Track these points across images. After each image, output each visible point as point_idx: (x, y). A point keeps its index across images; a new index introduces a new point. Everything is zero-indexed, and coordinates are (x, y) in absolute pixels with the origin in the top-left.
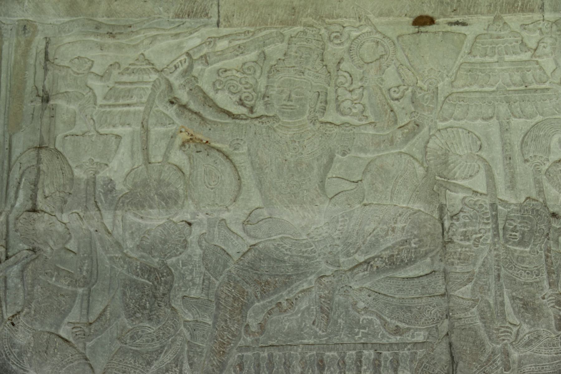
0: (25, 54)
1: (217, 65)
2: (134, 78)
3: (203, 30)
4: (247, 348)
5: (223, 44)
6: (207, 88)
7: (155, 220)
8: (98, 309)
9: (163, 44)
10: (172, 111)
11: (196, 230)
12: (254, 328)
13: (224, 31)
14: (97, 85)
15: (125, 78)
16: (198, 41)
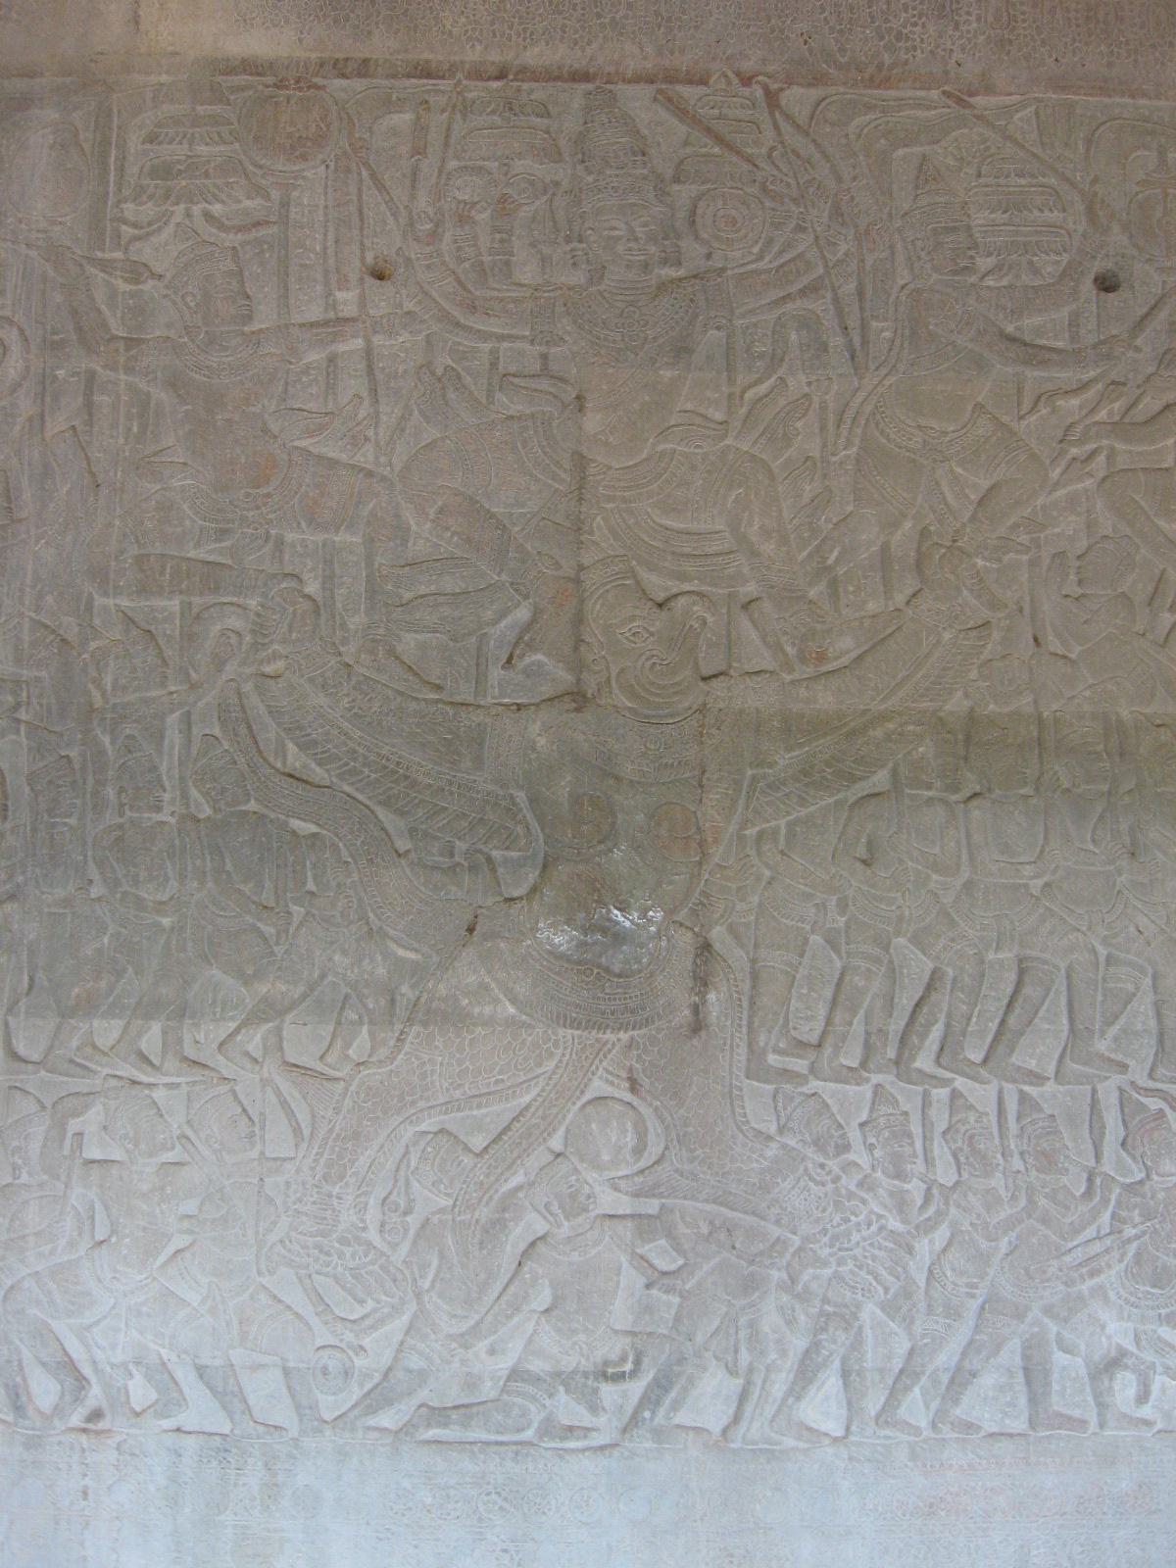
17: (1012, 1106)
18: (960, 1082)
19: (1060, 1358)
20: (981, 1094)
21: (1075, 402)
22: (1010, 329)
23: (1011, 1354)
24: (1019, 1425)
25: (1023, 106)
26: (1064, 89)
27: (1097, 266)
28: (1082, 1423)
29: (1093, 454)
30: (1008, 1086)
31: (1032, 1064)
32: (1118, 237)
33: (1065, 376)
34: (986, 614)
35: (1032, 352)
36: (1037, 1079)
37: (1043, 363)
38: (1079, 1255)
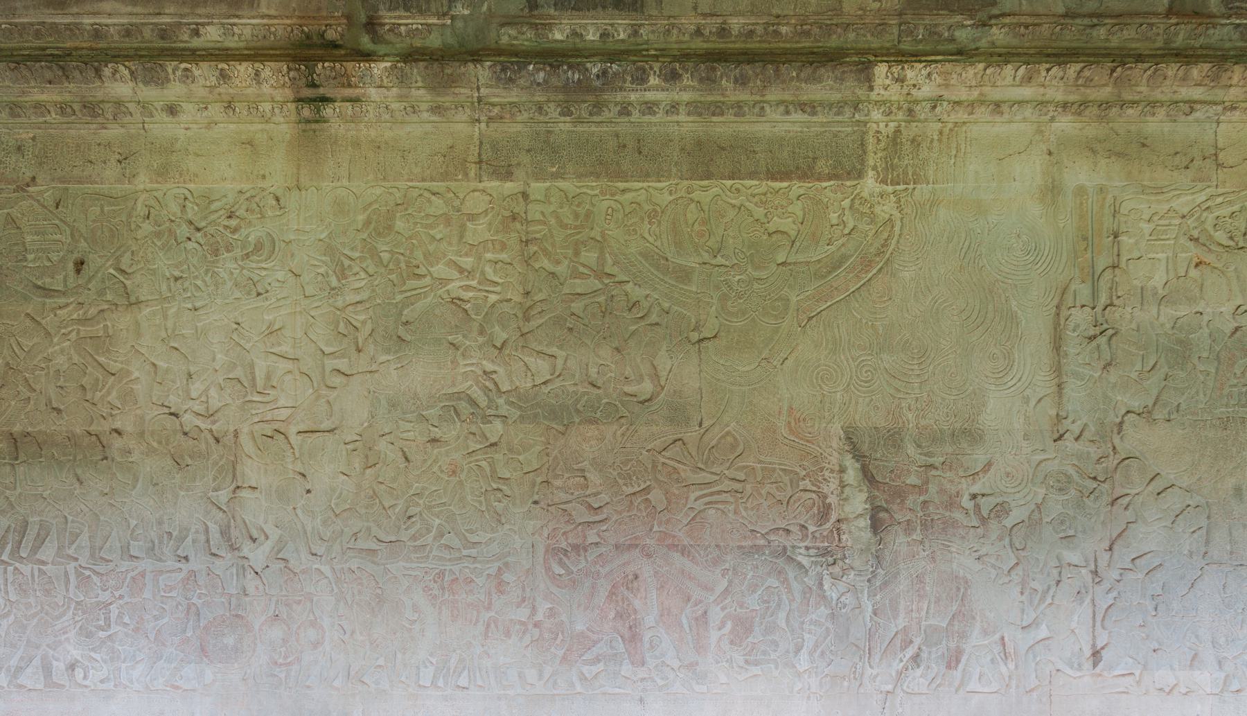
0: (1102, 207)
1: (1216, 214)
2: (1167, 222)
3: (1208, 190)
4: (1235, 386)
5: (1220, 200)
6: (1210, 229)
7: (1183, 310)
8: (1151, 363)
9: (1183, 199)
10: (1190, 244)
11: (1206, 318)
12: (1238, 373)
13: (1220, 191)
14: (1143, 225)
15: (1161, 222)
16: (1204, 198)
17: (36, 573)
18: (17, 565)
19: (55, 663)
20: (26, 569)
21: (65, 311)
22: (39, 283)
23: (37, 662)
24: (40, 686)
25: (47, 190)
26: (64, 182)
27: (76, 255)
28: (63, 686)
29: (70, 332)
30: (36, 567)
31: (44, 558)
32: (83, 244)
33: (62, 301)
34: (29, 394)
35: (47, 292)
36: (43, 563)
37: (51, 297)
38: (59, 626)
